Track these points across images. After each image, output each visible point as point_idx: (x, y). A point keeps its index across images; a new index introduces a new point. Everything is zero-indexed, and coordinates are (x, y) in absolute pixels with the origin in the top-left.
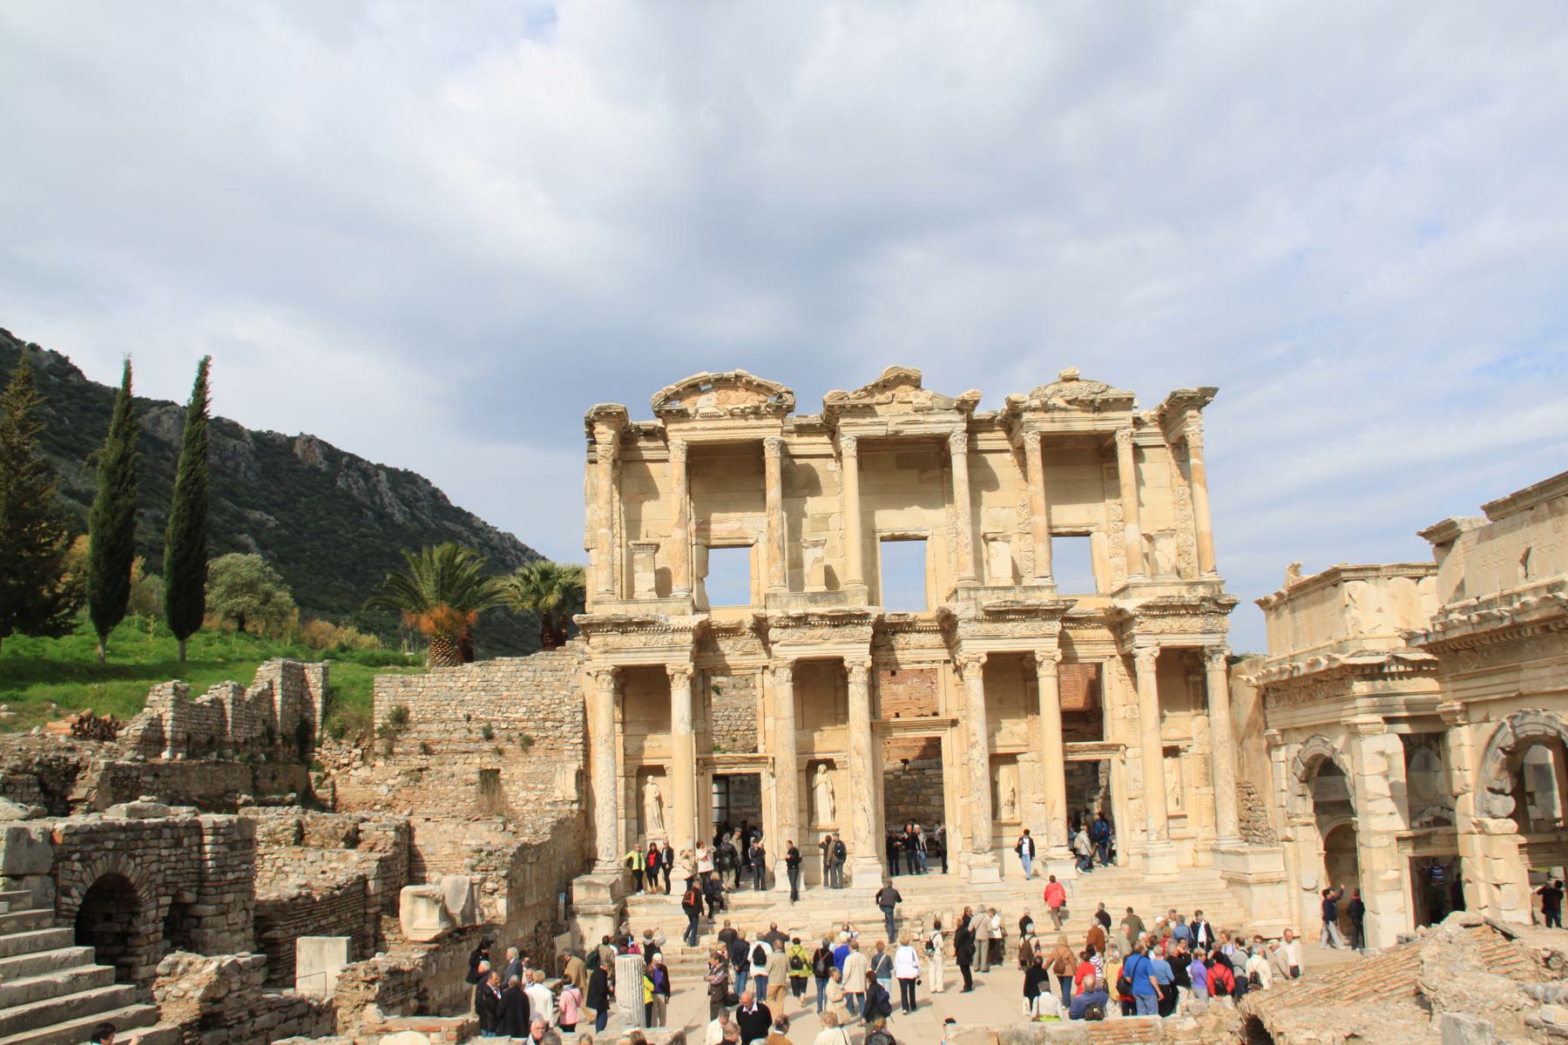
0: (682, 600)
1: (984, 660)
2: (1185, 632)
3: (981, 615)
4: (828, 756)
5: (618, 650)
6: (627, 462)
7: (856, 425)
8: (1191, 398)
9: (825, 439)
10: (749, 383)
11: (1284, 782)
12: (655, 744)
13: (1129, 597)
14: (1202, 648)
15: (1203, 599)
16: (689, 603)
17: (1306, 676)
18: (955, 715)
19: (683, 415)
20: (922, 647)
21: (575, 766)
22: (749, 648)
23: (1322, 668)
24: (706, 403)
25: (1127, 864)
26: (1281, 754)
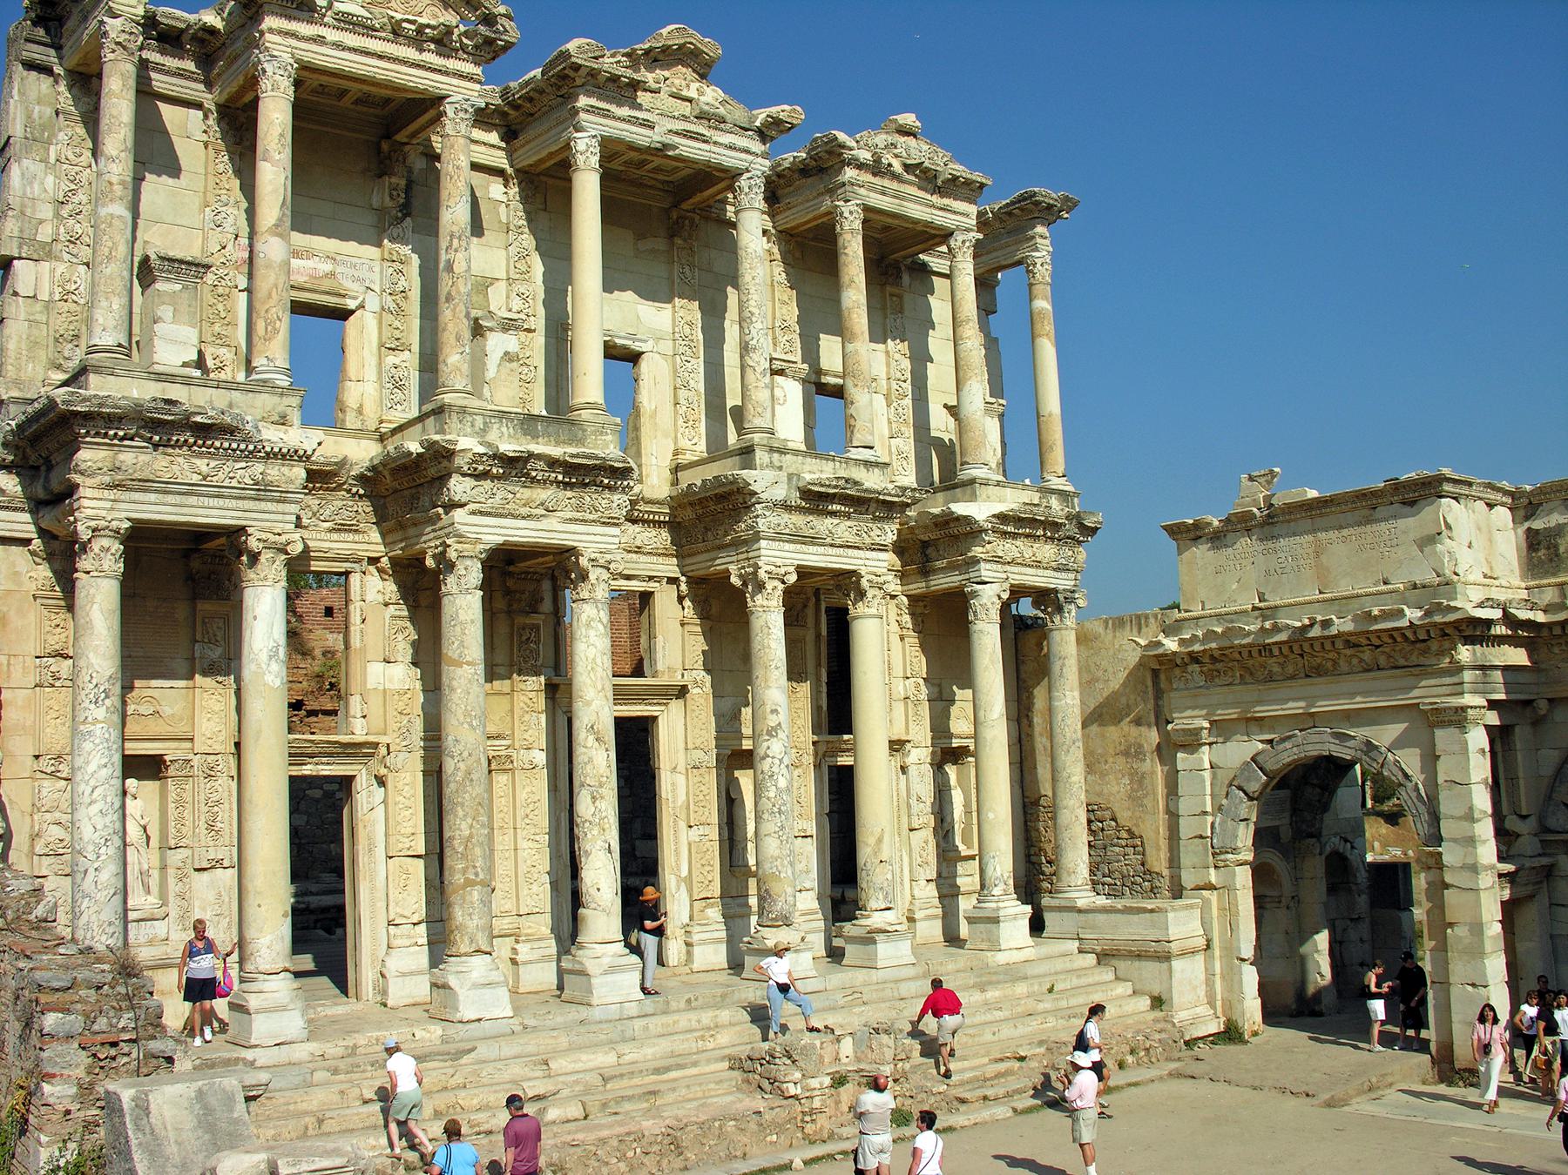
0: (283, 392)
1: (792, 578)
2: (1037, 564)
3: (795, 498)
5: (144, 484)
7: (606, 114)
8: (1050, 207)
11: (1208, 798)
12: (145, 709)
13: (973, 498)
14: (1055, 591)
17: (1339, 635)
18: (677, 680)
20: (638, 550)
23: (1404, 623)
26: (1205, 755)
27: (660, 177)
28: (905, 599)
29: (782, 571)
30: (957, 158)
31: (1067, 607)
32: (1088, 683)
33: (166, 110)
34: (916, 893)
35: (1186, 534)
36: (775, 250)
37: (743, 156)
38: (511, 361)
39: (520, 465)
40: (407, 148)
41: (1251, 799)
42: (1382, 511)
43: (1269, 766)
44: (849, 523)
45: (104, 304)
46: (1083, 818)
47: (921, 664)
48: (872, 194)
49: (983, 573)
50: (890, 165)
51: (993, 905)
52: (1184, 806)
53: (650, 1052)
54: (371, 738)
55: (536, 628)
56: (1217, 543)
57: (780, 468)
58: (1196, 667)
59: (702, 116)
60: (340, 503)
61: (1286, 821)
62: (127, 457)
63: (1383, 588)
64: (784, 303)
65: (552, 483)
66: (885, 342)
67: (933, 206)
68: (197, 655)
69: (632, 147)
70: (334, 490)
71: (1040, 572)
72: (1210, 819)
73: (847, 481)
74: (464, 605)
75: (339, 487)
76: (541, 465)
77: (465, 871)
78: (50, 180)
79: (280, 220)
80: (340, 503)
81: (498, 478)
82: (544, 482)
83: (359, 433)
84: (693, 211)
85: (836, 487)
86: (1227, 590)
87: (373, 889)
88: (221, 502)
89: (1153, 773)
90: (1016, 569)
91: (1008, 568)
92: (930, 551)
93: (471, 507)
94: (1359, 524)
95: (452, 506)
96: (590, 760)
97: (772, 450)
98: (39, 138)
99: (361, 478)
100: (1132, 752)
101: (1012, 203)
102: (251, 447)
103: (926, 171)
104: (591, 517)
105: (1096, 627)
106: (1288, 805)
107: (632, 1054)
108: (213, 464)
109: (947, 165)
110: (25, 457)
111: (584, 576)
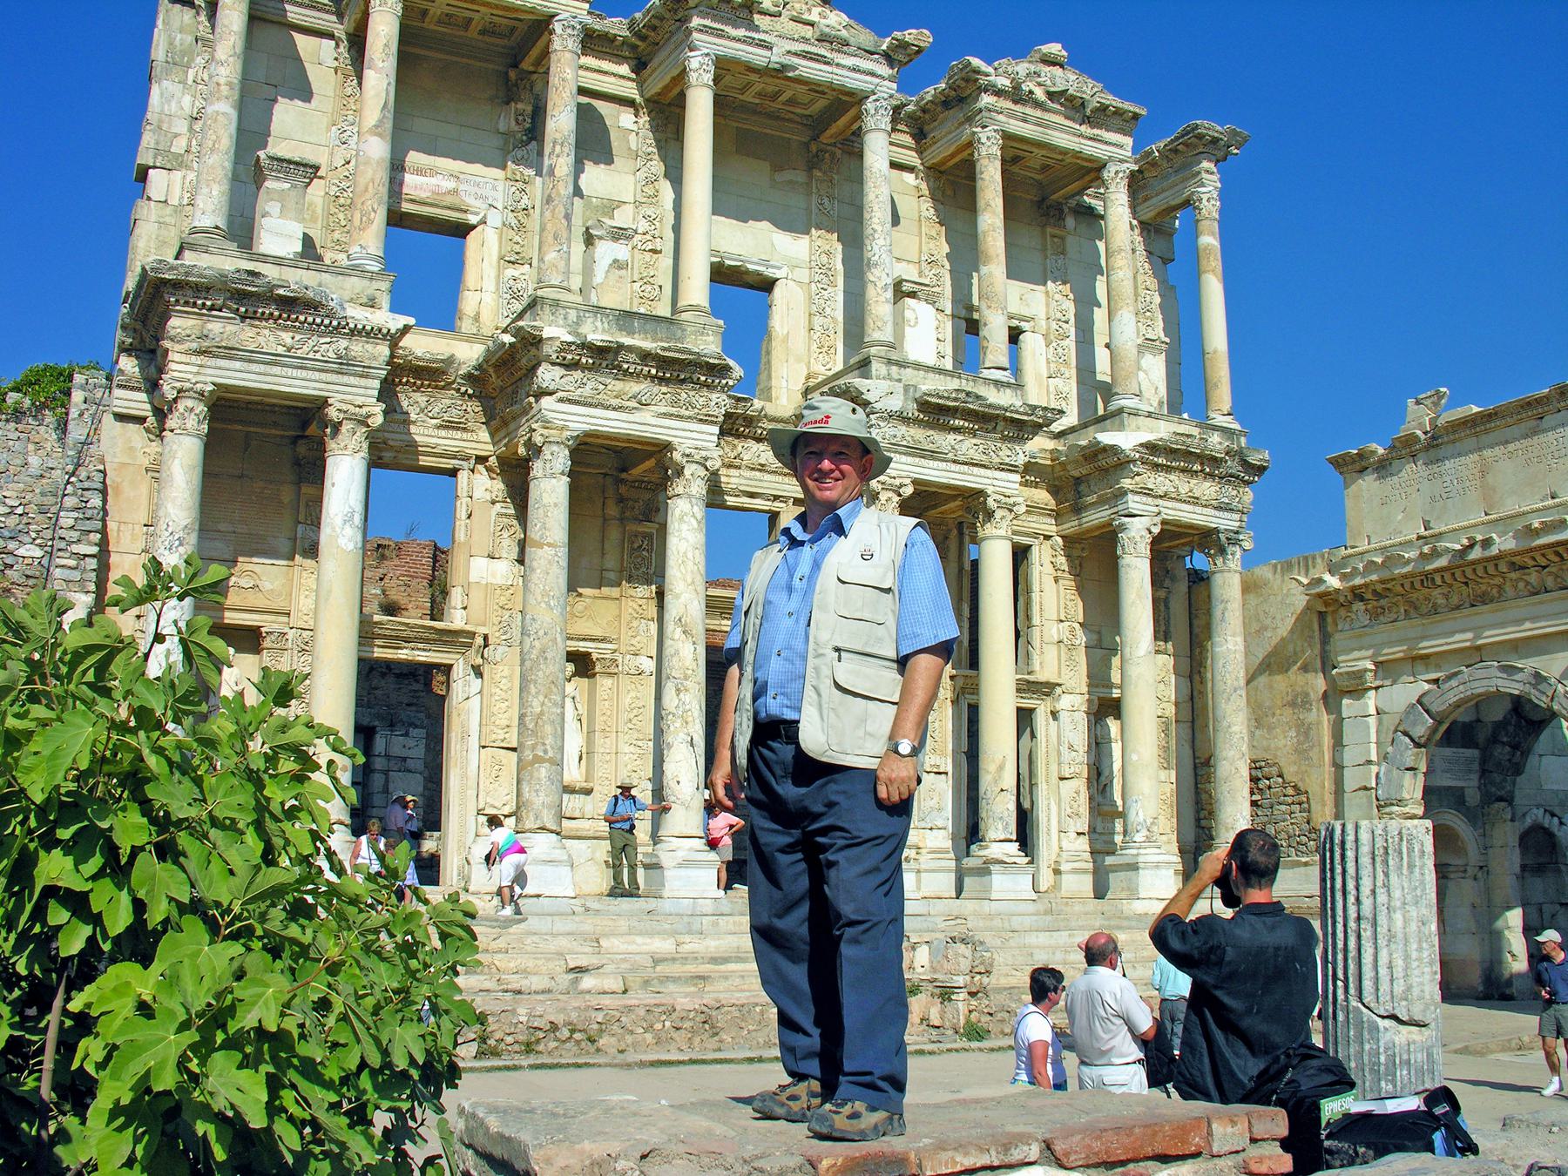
1: (908, 491)
2: (1195, 501)
3: (912, 410)
4: (583, 646)
5: (230, 352)
7: (720, 34)
8: (1215, 141)
9: (624, 69)
11: (1373, 747)
12: (244, 582)
13: (1121, 427)
14: (1217, 531)
17: (1500, 557)
22: (454, 415)
25: (1056, 887)
26: (1371, 701)
27: (798, 111)
28: (1059, 540)
29: (897, 482)
30: (1110, 88)
31: (1230, 549)
32: (1252, 632)
33: (299, 38)
34: (1065, 844)
35: (1353, 465)
36: (924, 186)
37: (868, 78)
38: (620, 268)
39: (611, 356)
40: (535, 76)
41: (1417, 745)
42: (1549, 420)
43: (1434, 708)
44: (975, 441)
45: (205, 190)
46: (1245, 773)
47: (1077, 609)
49: (1131, 504)
50: (1031, 92)
51: (1134, 852)
52: (1350, 756)
54: (468, 628)
55: (650, 536)
56: (1383, 473)
57: (899, 381)
58: (1359, 606)
59: (823, 39)
60: (448, 402)
61: (1476, 783)
62: (215, 327)
63: (1550, 502)
64: (932, 238)
65: (646, 377)
66: (1045, 284)
67: (1081, 136)
68: (299, 535)
69: (751, 68)
70: (443, 388)
71: (1198, 509)
72: (1374, 769)
73: (968, 394)
74: (551, 490)
75: (448, 386)
76: (632, 357)
77: (533, 748)
78: (187, 100)
79: (380, 121)
80: (448, 402)
81: (585, 368)
82: (637, 376)
83: (471, 339)
84: (834, 145)
85: (956, 400)
86: (1390, 519)
87: (464, 776)
88: (304, 373)
89: (1319, 723)
91: (1160, 502)
92: (1082, 488)
93: (560, 394)
94: (1526, 436)
95: (541, 393)
96: (677, 652)
97: (890, 362)
98: (178, 63)
99: (469, 377)
100: (1299, 702)
101: (1177, 138)
102: (335, 323)
103: (1071, 99)
104: (687, 413)
105: (1264, 572)
106: (1476, 766)
107: (692, 945)
108: (298, 337)
109: (1091, 91)
110: (142, 341)
111: (679, 472)
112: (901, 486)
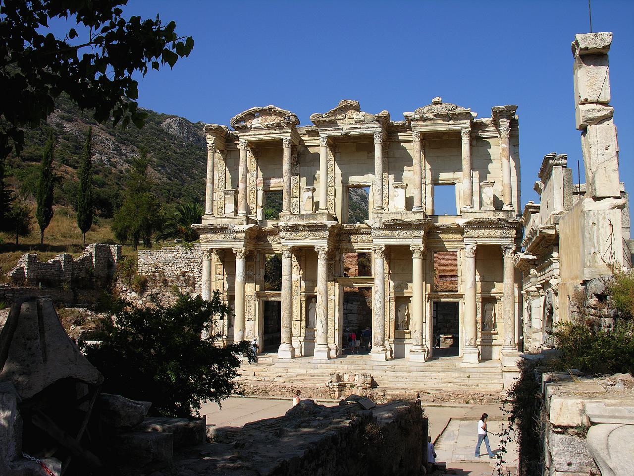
1: (383, 249)
2: (491, 237)
3: (382, 226)
5: (212, 241)
6: (229, 151)
8: (500, 112)
10: (275, 111)
15: (500, 220)
16: (244, 219)
19: (245, 129)
20: (364, 242)
21: (197, 295)
24: (256, 122)
39: (295, 227)
48: (422, 127)
53: (316, 372)
59: (356, 122)
62: (208, 236)
71: (492, 239)
85: (393, 222)
90: (481, 239)
91: (477, 239)
93: (286, 238)
112: (381, 248)
